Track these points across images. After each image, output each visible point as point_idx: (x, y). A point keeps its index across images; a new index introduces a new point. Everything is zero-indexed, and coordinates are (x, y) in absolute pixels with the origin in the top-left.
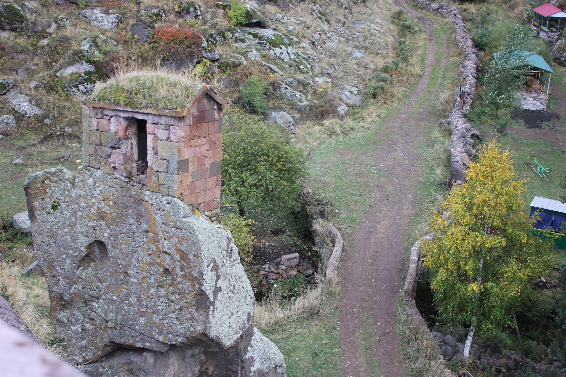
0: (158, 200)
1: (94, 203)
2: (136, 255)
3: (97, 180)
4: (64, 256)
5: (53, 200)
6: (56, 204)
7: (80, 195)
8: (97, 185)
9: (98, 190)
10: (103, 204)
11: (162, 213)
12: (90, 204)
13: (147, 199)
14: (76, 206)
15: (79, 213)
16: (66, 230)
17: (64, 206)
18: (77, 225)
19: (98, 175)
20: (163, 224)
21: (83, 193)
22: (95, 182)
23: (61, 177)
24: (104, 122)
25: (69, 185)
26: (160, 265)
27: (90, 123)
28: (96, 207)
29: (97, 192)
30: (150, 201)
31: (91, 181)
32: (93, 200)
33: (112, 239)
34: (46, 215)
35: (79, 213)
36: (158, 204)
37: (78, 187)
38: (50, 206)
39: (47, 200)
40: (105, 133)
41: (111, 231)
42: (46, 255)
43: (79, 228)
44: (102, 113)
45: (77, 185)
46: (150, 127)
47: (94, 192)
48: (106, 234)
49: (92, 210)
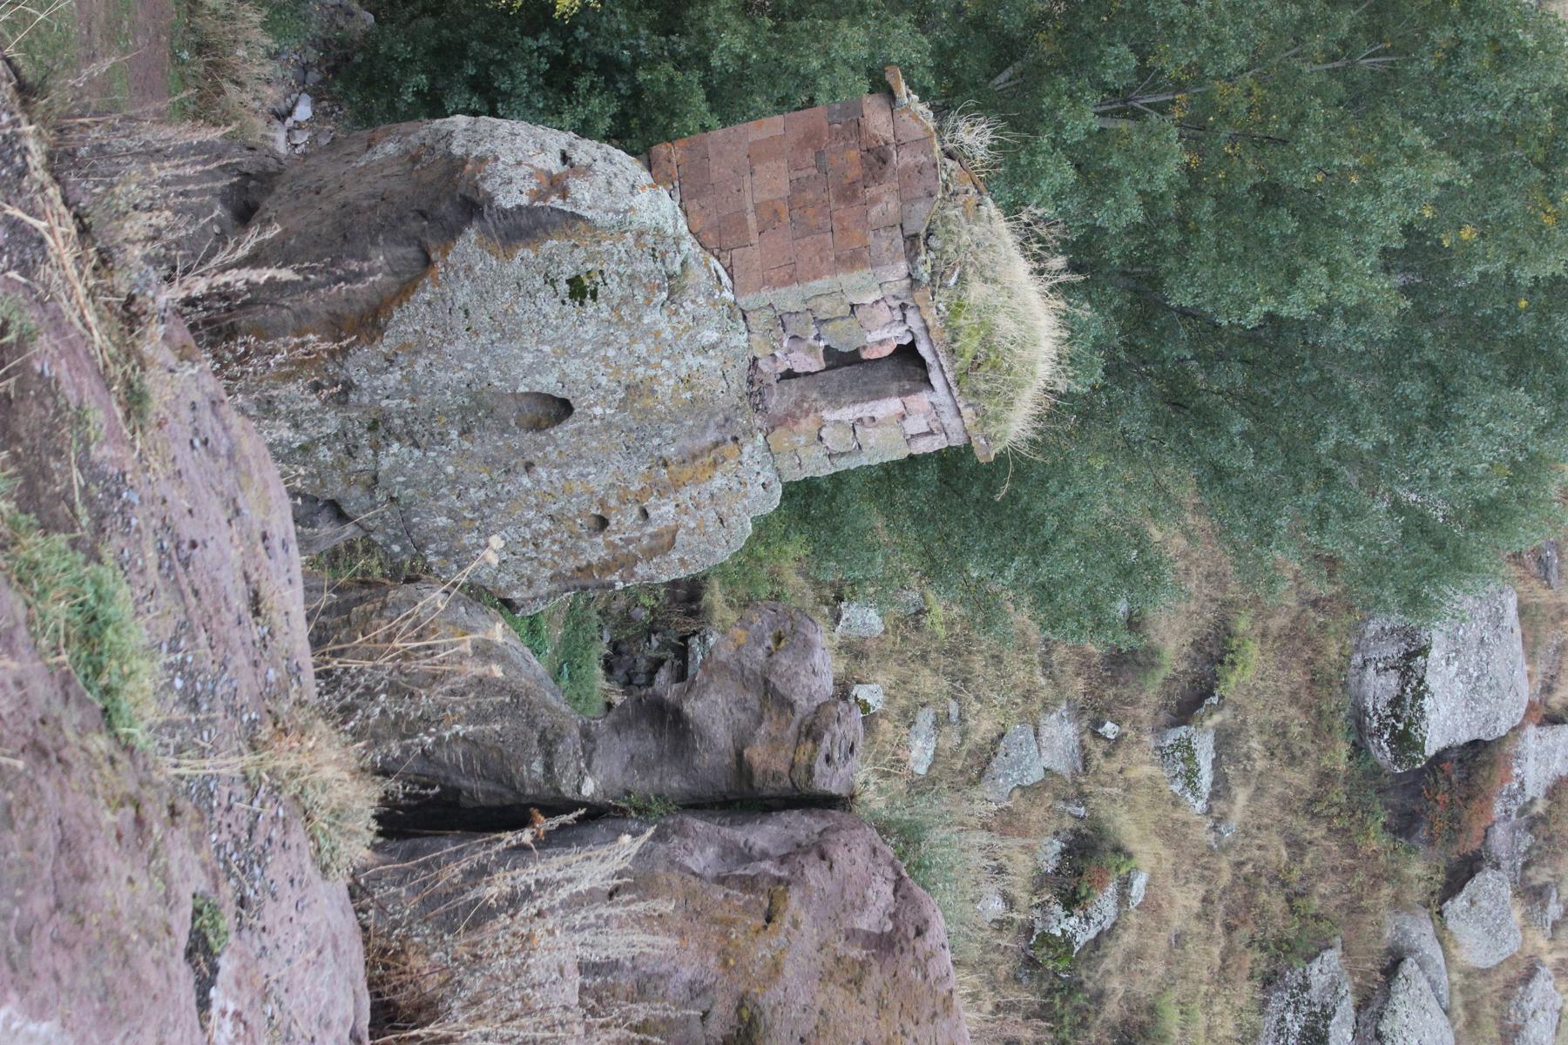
0: (757, 468)
1: (659, 365)
2: (592, 469)
3: (722, 346)
4: (470, 366)
5: (590, 266)
6: (587, 282)
7: (657, 334)
8: (711, 353)
9: (700, 359)
10: (672, 382)
11: (734, 485)
12: (652, 361)
13: (747, 449)
14: (624, 339)
15: (611, 353)
16: (547, 349)
17: (605, 315)
18: (577, 361)
19: (734, 343)
20: (712, 495)
21: (668, 335)
22: (713, 346)
23: (661, 248)
24: (884, 314)
25: (665, 295)
26: (602, 503)
27: (861, 289)
28: (651, 373)
29: (692, 361)
30: (745, 458)
31: (710, 335)
32: (666, 363)
33: (597, 423)
34: (539, 281)
35: (611, 353)
36: (750, 471)
37: (675, 319)
38: (569, 271)
39: (580, 254)
40: (856, 325)
41: (613, 416)
42: (438, 333)
43: (573, 367)
44: (903, 307)
45: (676, 313)
46: (921, 400)
47: (689, 356)
48: (598, 411)
49: (641, 370)
